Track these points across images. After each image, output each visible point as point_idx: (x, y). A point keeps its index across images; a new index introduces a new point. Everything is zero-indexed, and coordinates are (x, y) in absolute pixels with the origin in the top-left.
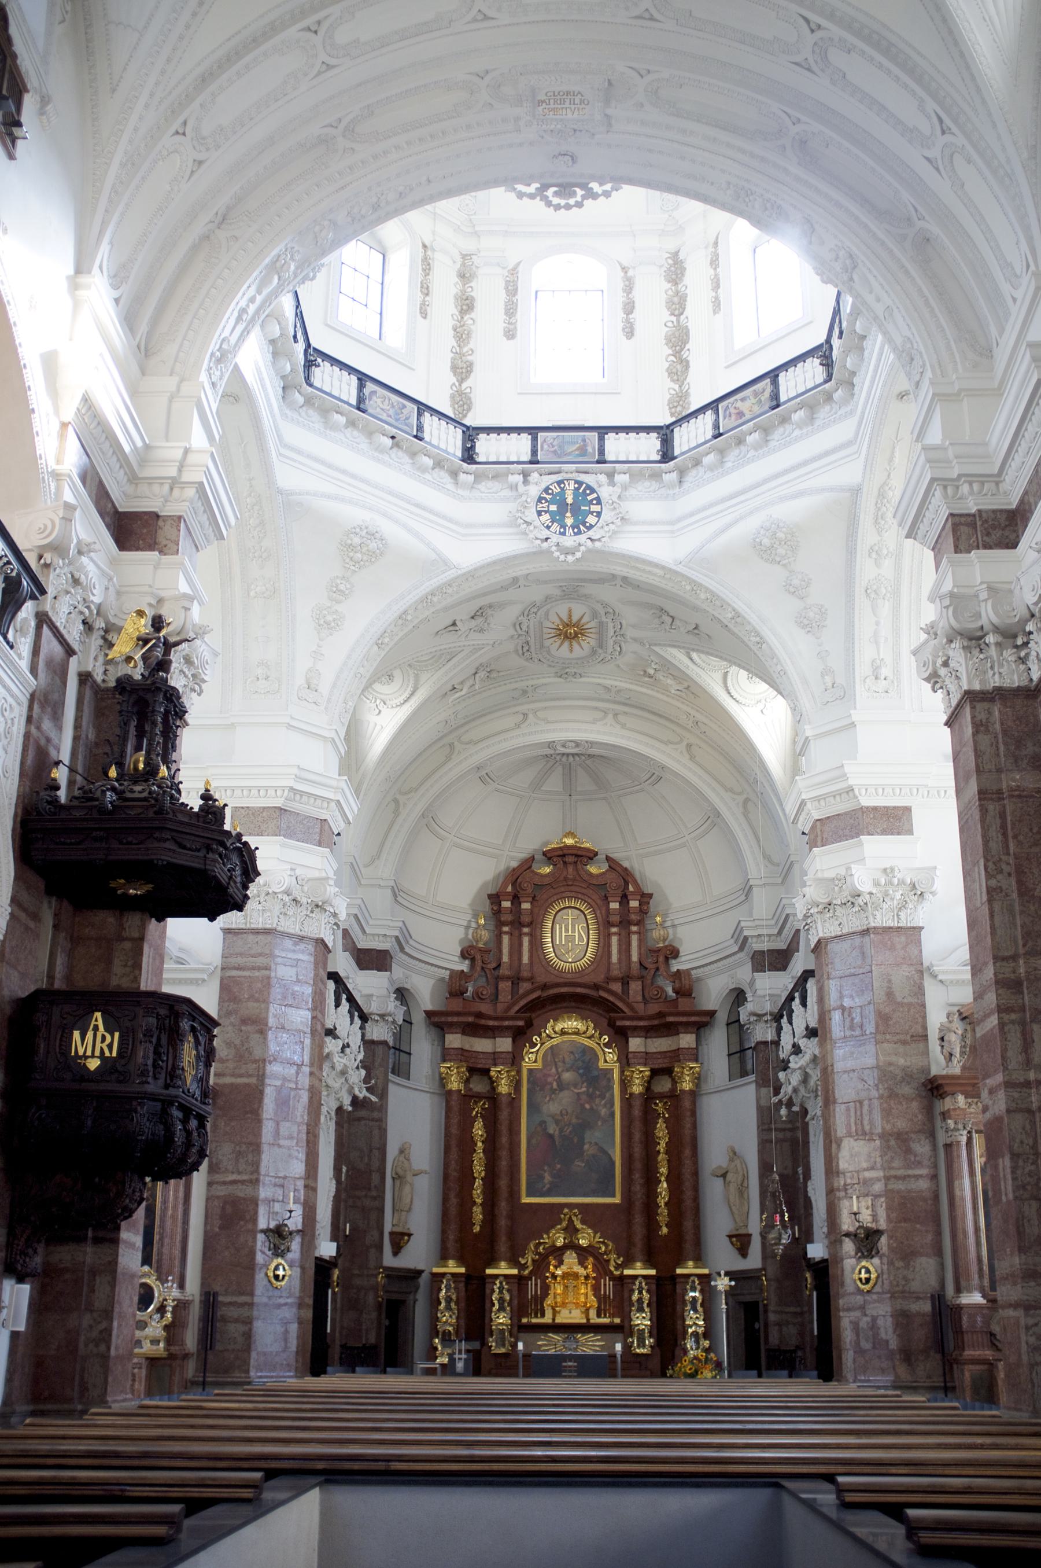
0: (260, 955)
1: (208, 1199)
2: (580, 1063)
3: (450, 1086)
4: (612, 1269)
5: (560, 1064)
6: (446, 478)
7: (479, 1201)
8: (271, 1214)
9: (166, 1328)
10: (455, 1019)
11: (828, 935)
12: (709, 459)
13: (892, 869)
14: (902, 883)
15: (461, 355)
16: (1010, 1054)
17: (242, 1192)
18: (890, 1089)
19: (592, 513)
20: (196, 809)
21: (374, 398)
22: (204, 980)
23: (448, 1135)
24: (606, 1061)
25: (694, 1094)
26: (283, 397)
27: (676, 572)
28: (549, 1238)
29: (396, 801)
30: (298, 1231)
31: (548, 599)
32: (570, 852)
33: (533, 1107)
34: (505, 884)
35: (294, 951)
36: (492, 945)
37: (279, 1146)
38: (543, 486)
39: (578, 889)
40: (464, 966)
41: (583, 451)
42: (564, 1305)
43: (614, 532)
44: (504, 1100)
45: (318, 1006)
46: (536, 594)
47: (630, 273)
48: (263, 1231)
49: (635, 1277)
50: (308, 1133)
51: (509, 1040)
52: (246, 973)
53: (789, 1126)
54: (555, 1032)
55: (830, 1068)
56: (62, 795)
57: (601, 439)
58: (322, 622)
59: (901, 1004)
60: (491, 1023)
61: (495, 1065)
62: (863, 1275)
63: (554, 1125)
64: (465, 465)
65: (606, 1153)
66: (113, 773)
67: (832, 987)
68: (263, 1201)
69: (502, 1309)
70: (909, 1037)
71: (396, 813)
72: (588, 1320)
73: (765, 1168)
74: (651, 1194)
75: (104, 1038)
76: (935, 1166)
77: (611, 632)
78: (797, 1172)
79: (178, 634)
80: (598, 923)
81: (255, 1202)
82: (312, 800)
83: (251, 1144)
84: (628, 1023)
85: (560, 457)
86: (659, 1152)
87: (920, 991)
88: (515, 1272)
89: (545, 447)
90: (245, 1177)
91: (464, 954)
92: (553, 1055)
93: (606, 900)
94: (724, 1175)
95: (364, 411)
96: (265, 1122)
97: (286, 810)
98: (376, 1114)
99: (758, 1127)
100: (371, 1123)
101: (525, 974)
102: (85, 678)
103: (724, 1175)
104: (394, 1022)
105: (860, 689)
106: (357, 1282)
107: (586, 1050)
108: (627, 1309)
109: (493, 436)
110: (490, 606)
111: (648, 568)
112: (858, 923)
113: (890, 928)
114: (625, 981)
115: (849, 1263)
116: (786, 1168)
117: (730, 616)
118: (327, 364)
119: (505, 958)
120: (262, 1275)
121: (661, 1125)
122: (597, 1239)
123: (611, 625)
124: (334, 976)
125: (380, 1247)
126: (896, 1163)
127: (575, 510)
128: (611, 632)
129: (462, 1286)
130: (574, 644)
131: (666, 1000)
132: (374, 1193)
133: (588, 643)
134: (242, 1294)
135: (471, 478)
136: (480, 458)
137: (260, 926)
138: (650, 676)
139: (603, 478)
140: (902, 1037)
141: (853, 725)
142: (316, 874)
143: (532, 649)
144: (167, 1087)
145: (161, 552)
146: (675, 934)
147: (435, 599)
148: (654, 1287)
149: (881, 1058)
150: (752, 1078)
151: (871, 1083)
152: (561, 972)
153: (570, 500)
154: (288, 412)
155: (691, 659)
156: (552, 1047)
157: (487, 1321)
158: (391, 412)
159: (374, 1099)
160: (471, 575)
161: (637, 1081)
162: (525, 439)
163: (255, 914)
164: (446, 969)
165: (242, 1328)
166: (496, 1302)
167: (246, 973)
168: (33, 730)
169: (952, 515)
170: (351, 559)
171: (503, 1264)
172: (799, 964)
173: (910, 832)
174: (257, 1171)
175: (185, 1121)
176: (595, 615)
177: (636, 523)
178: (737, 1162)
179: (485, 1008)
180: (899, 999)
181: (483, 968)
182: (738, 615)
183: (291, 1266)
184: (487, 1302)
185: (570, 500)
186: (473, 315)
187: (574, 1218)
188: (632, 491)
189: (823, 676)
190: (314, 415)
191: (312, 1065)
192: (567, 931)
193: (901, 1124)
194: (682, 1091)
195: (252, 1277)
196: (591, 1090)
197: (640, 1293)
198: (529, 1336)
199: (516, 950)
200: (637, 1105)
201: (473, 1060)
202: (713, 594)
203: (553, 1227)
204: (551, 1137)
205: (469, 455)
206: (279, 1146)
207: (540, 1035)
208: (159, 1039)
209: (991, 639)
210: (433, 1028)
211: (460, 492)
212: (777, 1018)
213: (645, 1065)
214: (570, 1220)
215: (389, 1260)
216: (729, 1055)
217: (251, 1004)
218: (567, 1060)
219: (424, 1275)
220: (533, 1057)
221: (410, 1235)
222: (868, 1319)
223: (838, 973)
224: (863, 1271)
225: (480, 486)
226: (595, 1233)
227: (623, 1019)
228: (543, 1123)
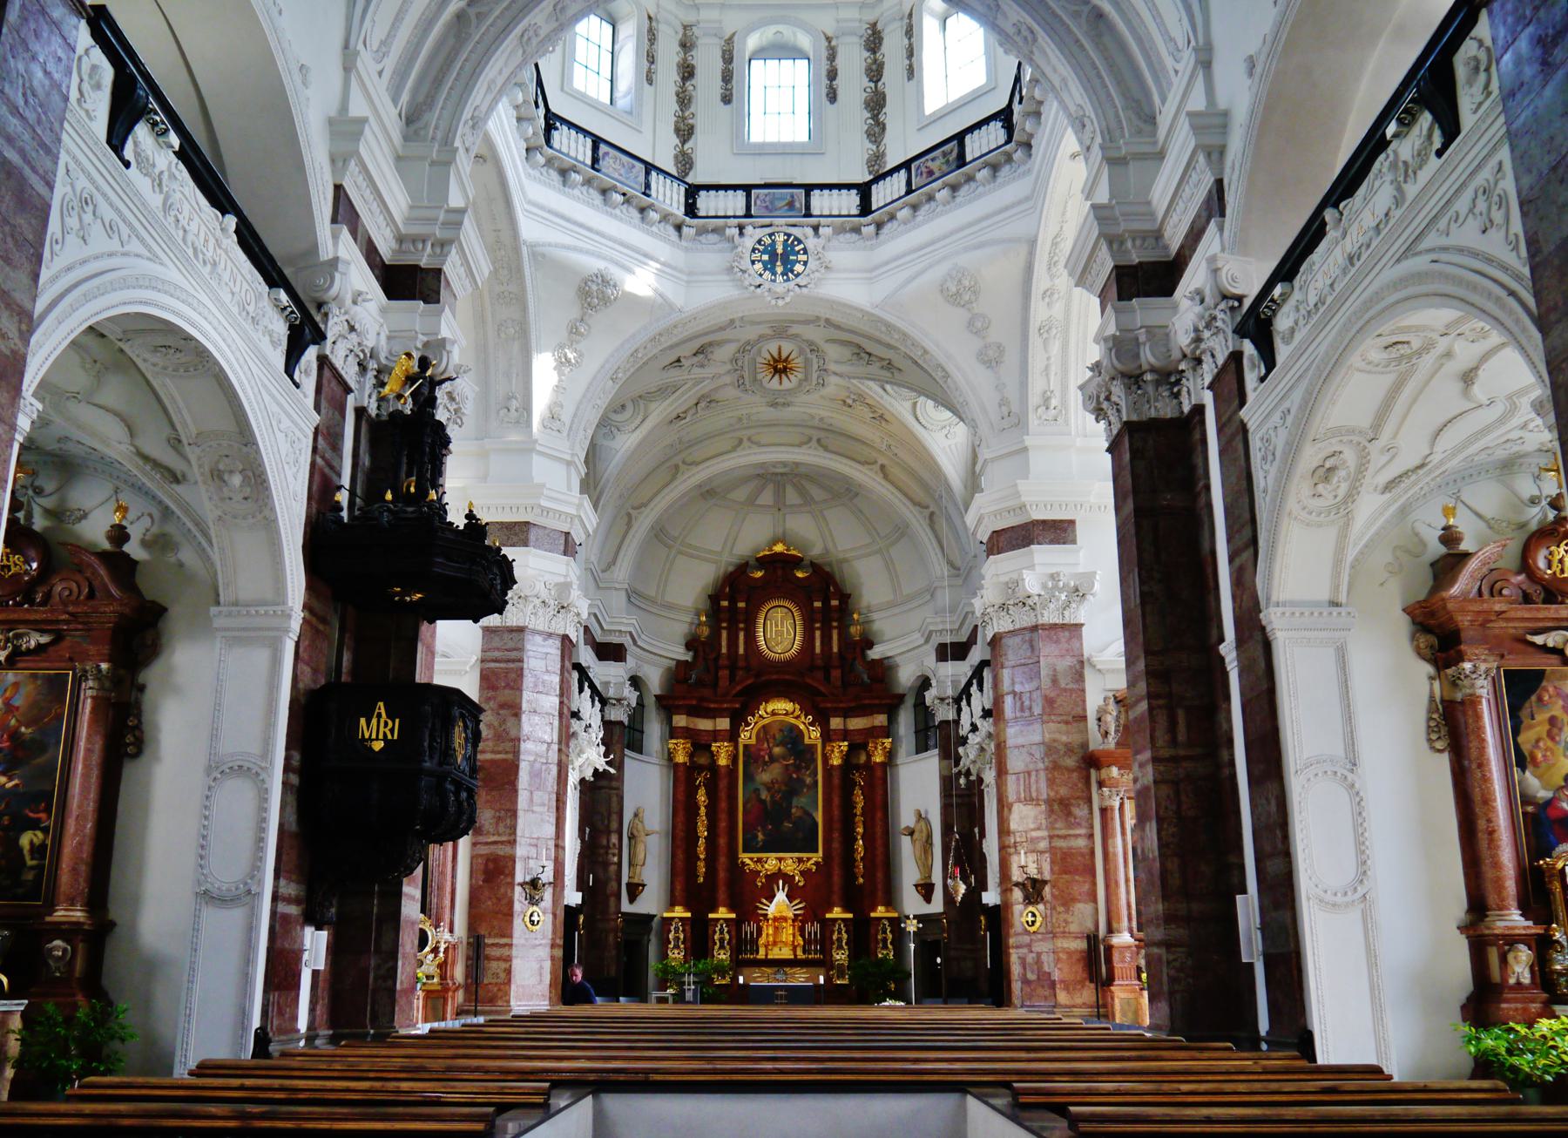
1: (473, 858)
7: (702, 856)
8: (527, 870)
11: (1002, 630)
12: (904, 214)
13: (1058, 574)
15: (684, 119)
16: (1158, 733)
17: (502, 851)
18: (1054, 762)
20: (462, 527)
27: (873, 315)
29: (629, 515)
31: (761, 338)
33: (748, 777)
40: (688, 657)
41: (791, 205)
42: (775, 943)
43: (819, 279)
44: (723, 771)
45: (564, 692)
46: (751, 333)
48: (521, 885)
49: (835, 920)
51: (728, 720)
52: (502, 665)
56: (345, 514)
57: (808, 196)
59: (1065, 690)
60: (712, 706)
64: (687, 219)
65: (810, 815)
66: (389, 496)
67: (1006, 674)
70: (1070, 719)
71: (629, 525)
72: (795, 955)
75: (386, 724)
76: (1092, 827)
77: (815, 367)
79: (442, 374)
83: (508, 810)
84: (829, 705)
85: (771, 211)
87: (1079, 677)
90: (504, 838)
91: (689, 646)
94: (911, 833)
95: (598, 171)
96: (520, 792)
98: (614, 784)
102: (360, 412)
104: (629, 705)
105: (1031, 416)
109: (712, 193)
110: (711, 344)
115: (1018, 908)
118: (565, 128)
119: (724, 650)
121: (858, 791)
123: (815, 360)
124: (577, 667)
126: (1057, 826)
127: (785, 256)
128: (815, 367)
129: (687, 928)
130: (784, 376)
134: (503, 936)
135: (693, 231)
136: (702, 213)
139: (810, 231)
140: (1065, 718)
141: (1025, 449)
142: (562, 580)
143: (747, 383)
144: (440, 764)
145: (426, 302)
147: (662, 339)
148: (851, 928)
149: (1047, 735)
150: (936, 751)
151: (1038, 756)
153: (780, 250)
156: (764, 727)
158: (622, 171)
159: (612, 771)
162: (741, 195)
165: (503, 965)
168: (319, 460)
169: (1116, 267)
171: (722, 909)
172: (976, 655)
173: (1074, 542)
174: (514, 833)
175: (457, 794)
176: (801, 352)
178: (922, 823)
180: (1063, 686)
182: (926, 352)
183: (544, 913)
185: (780, 250)
188: (834, 243)
189: (1000, 406)
191: (560, 742)
192: (777, 626)
193: (1063, 791)
197: (840, 933)
198: (746, 971)
202: (905, 334)
204: (763, 802)
207: (753, 716)
208: (433, 724)
209: (1148, 377)
212: (957, 701)
215: (626, 907)
216: (916, 732)
217: (507, 692)
220: (748, 734)
221: (644, 886)
223: (1013, 663)
228: (757, 791)
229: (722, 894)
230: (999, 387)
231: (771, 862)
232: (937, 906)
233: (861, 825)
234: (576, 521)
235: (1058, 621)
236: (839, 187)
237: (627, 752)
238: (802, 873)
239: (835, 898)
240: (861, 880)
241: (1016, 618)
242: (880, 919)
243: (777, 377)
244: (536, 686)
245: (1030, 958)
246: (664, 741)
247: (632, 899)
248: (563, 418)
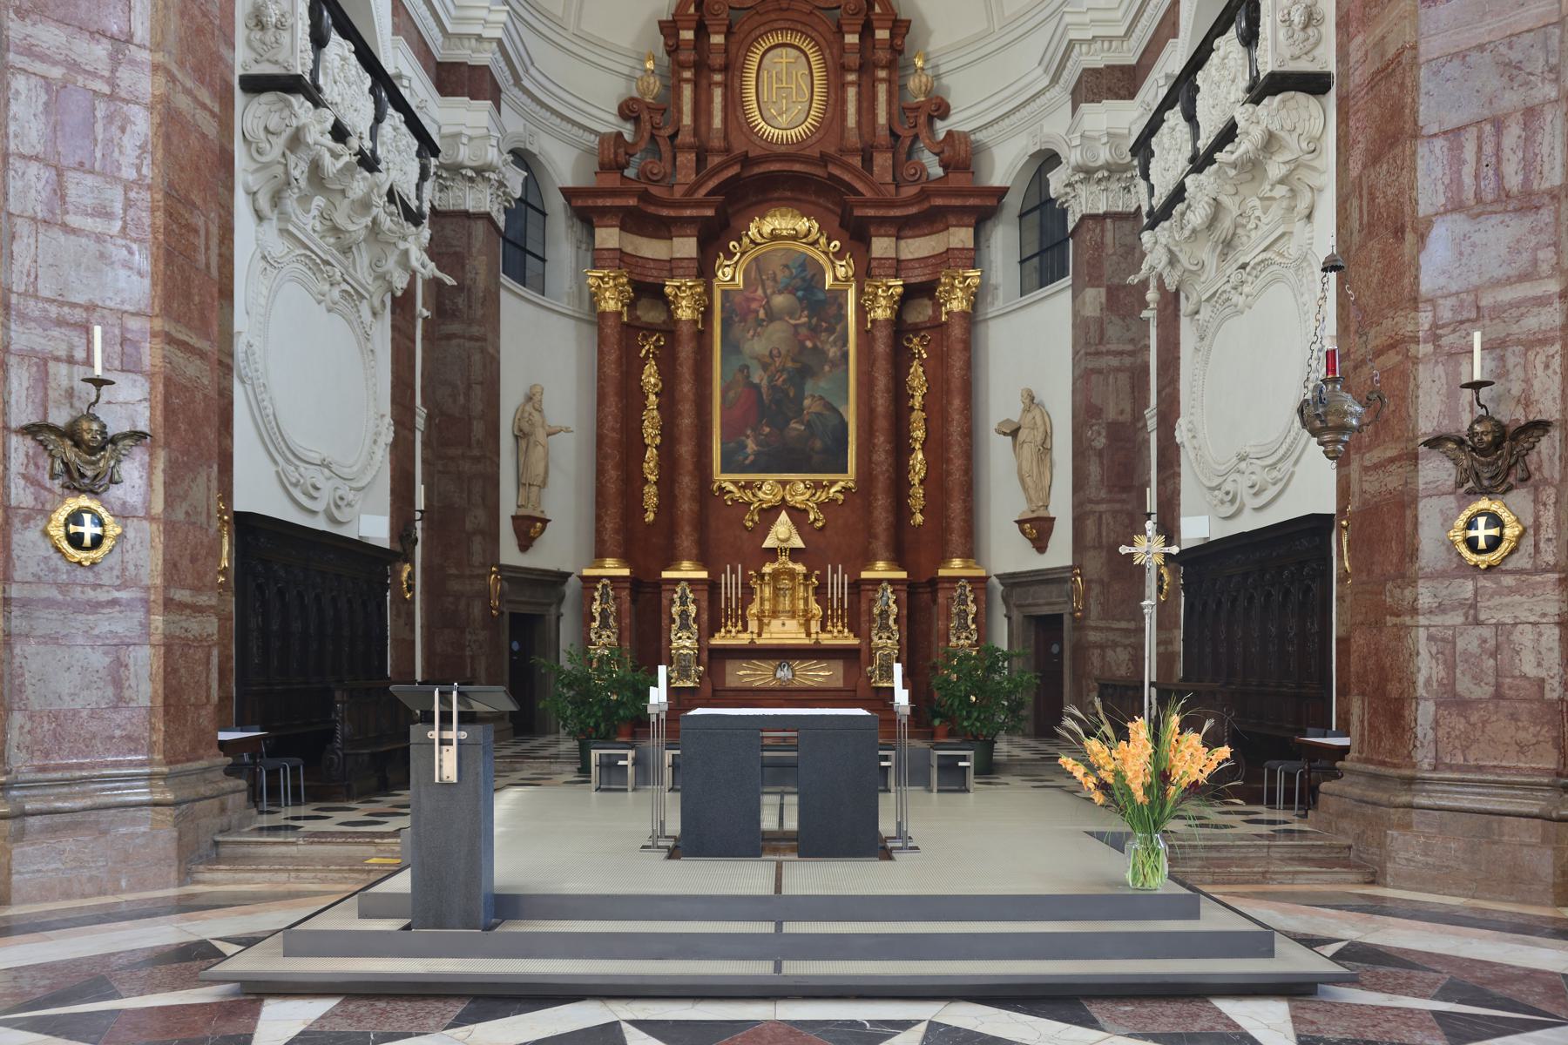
2: (798, 282)
5: (769, 283)
7: (652, 478)
23: (601, 377)
25: (971, 319)
30: (137, 436)
33: (730, 347)
39: (796, 16)
40: (628, 130)
44: (685, 330)
48: (31, 430)
49: (879, 581)
51: (693, 241)
53: (1129, 347)
54: (761, 235)
55: (1407, 55)
60: (665, 212)
61: (672, 277)
63: (761, 372)
69: (685, 626)
73: (1085, 414)
84: (871, 212)
86: (912, 409)
91: (628, 110)
92: (759, 270)
93: (840, 32)
94: (1014, 433)
98: (475, 330)
99: (1075, 353)
100: (468, 344)
101: (717, 143)
103: (1014, 433)
106: (455, 586)
107: (807, 263)
108: (864, 626)
116: (1122, 412)
119: (687, 120)
129: (625, 594)
132: (476, 452)
148: (904, 596)
150: (1067, 281)
156: (756, 259)
157: (664, 643)
164: (596, 133)
166: (677, 617)
171: (686, 564)
178: (1036, 412)
179: (654, 190)
181: (653, 137)
184: (664, 616)
192: (779, 80)
196: (814, 321)
199: (701, 109)
201: (638, 270)
204: (757, 387)
207: (739, 240)
210: (578, 224)
216: (1022, 262)
218: (780, 276)
219: (570, 579)
221: (545, 521)
222: (1487, 632)
228: (745, 368)
229: (686, 541)
231: (768, 488)
232: (1060, 553)
238: (821, 506)
239: (879, 545)
240: (919, 518)
242: (956, 579)
245: (1469, 641)
246: (580, 278)
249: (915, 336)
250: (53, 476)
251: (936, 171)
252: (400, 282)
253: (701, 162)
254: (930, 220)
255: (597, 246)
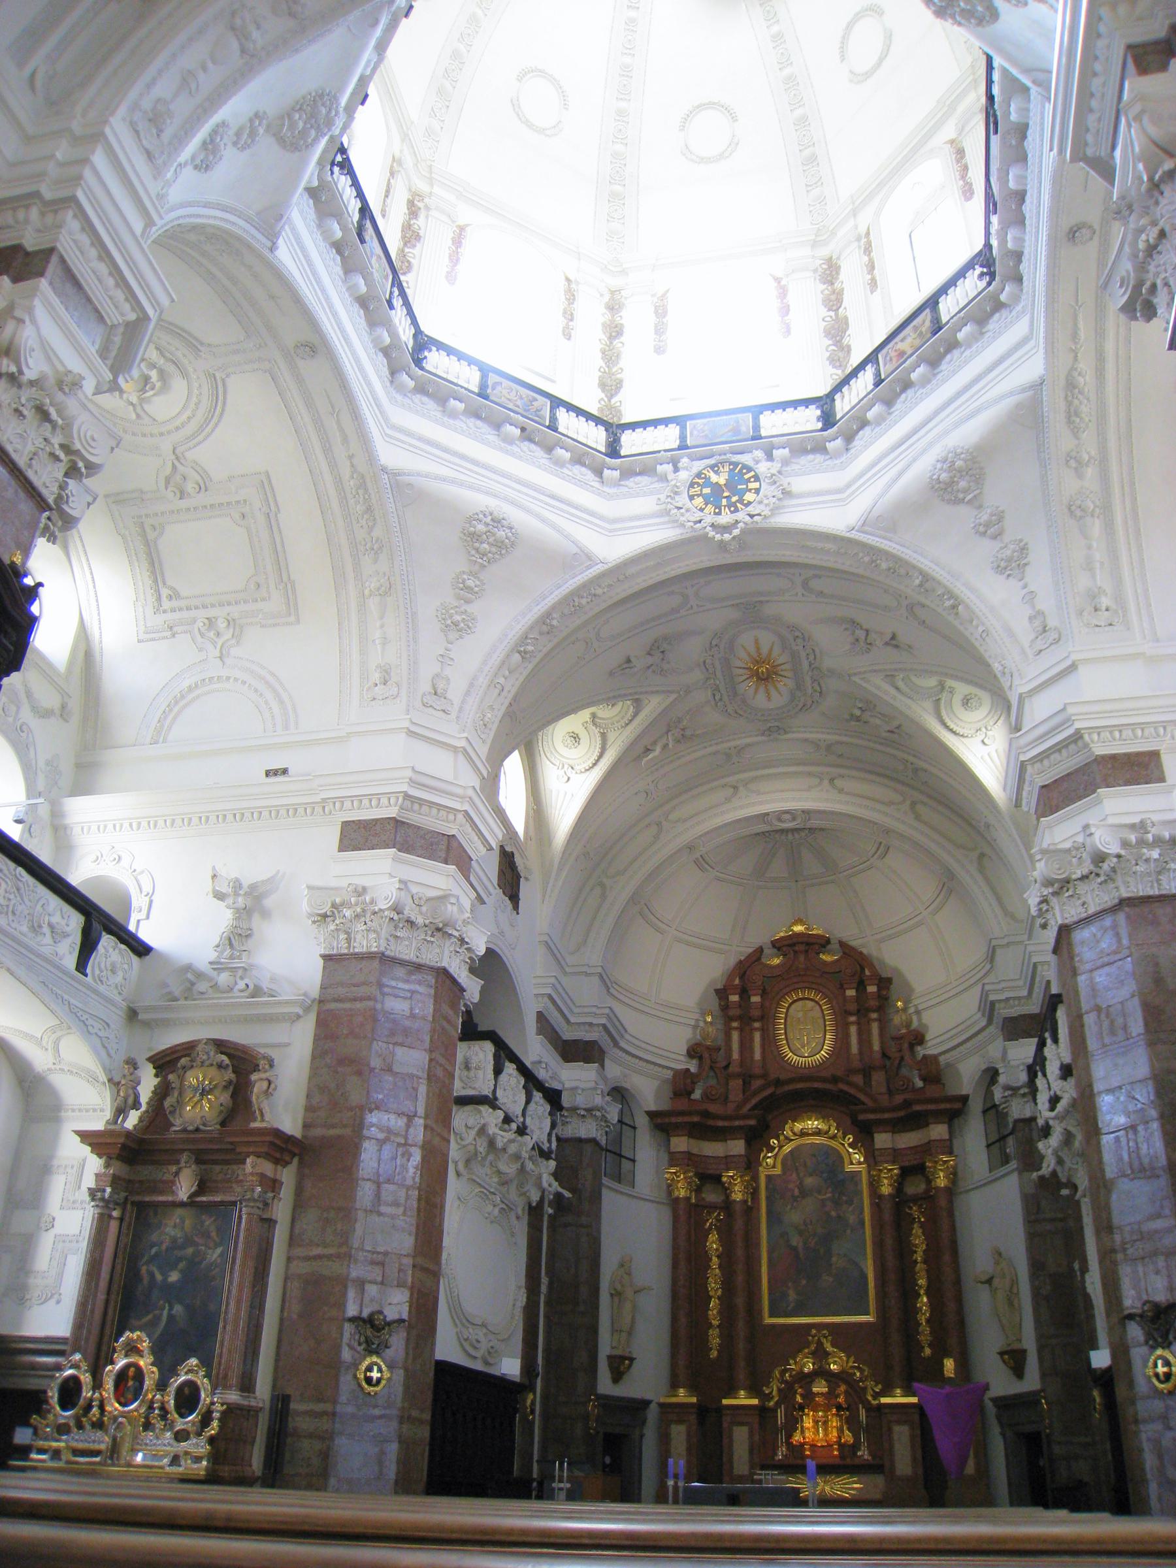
0: (364, 984)
3: (676, 1193)
4: (870, 1398)
6: (589, 476)
7: (715, 1323)
9: (212, 1440)
10: (680, 1119)
14: (1158, 842)
15: (611, 374)
19: (750, 490)
21: (499, 388)
22: (299, 1017)
23: (675, 1248)
24: (852, 1163)
25: (951, 1192)
26: (392, 382)
28: (796, 1363)
29: (603, 886)
30: (401, 1321)
32: (800, 940)
33: (774, 1218)
34: (730, 977)
35: (407, 981)
36: (720, 1042)
37: (380, 1214)
38: (695, 470)
40: (693, 1067)
44: (738, 1208)
45: (441, 1051)
47: (783, 283)
48: (352, 1320)
50: (419, 1200)
52: (347, 1005)
53: (1060, 1215)
54: (795, 1134)
58: (449, 622)
60: (720, 1123)
61: (728, 1170)
62: (1161, 1369)
64: (607, 459)
68: (354, 1281)
73: (1037, 1266)
74: (909, 1312)
78: (1072, 1270)
80: (834, 1013)
81: (343, 1282)
82: (434, 811)
84: (871, 1116)
86: (916, 1262)
88: (755, 1402)
89: (695, 433)
90: (331, 1251)
91: (693, 1052)
93: (842, 988)
95: (486, 397)
97: (403, 823)
98: (584, 1220)
104: (604, 1118)
107: (829, 1152)
110: (665, 638)
111: (820, 545)
112: (1106, 898)
113: (1150, 897)
114: (867, 1072)
117: (917, 582)
119: (735, 1056)
120: (349, 1377)
121: (917, 1230)
122: (850, 1364)
123: (803, 654)
125: (592, 1369)
131: (915, 1090)
132: (582, 1308)
133: (785, 685)
134: (320, 1400)
135: (616, 474)
137: (365, 950)
138: (858, 719)
139: (759, 454)
142: (440, 893)
143: (725, 698)
146: (920, 1020)
150: (1013, 1164)
152: (796, 1067)
154: (399, 398)
155: (897, 688)
158: (519, 403)
160: (620, 571)
161: (886, 1181)
163: (359, 937)
167: (347, 1005)
170: (477, 550)
173: (1162, 779)
177: (800, 496)
179: (714, 1108)
181: (712, 1068)
182: (926, 577)
183: (391, 1367)
186: (623, 339)
187: (824, 1341)
190: (431, 404)
191: (426, 1117)
194: (937, 1189)
195: (336, 1377)
196: (837, 1195)
199: (746, 1045)
200: (887, 1207)
203: (800, 1351)
204: (795, 1249)
205: (613, 450)
206: (380, 1214)
211: (605, 489)
213: (893, 1163)
214: (820, 1343)
215: (605, 1385)
216: (988, 1146)
219: (653, 1406)
221: (632, 1360)
223: (1088, 967)
224: (1160, 1362)
225: (627, 483)
226: (848, 1357)
227: (865, 1111)
230: (1030, 597)
233: (923, 1273)
234: (460, 816)
235: (1155, 892)
236: (795, 404)
237: (605, 1180)
240: (928, 1351)
241: (1089, 899)
243: (762, 689)
244: (392, 1033)
247: (618, 1376)
248: (449, 695)
249: (915, 1204)
250: (360, 1344)
251: (919, 1084)
252: (535, 1197)
253: (746, 1084)
254: (916, 1121)
255: (673, 1149)
